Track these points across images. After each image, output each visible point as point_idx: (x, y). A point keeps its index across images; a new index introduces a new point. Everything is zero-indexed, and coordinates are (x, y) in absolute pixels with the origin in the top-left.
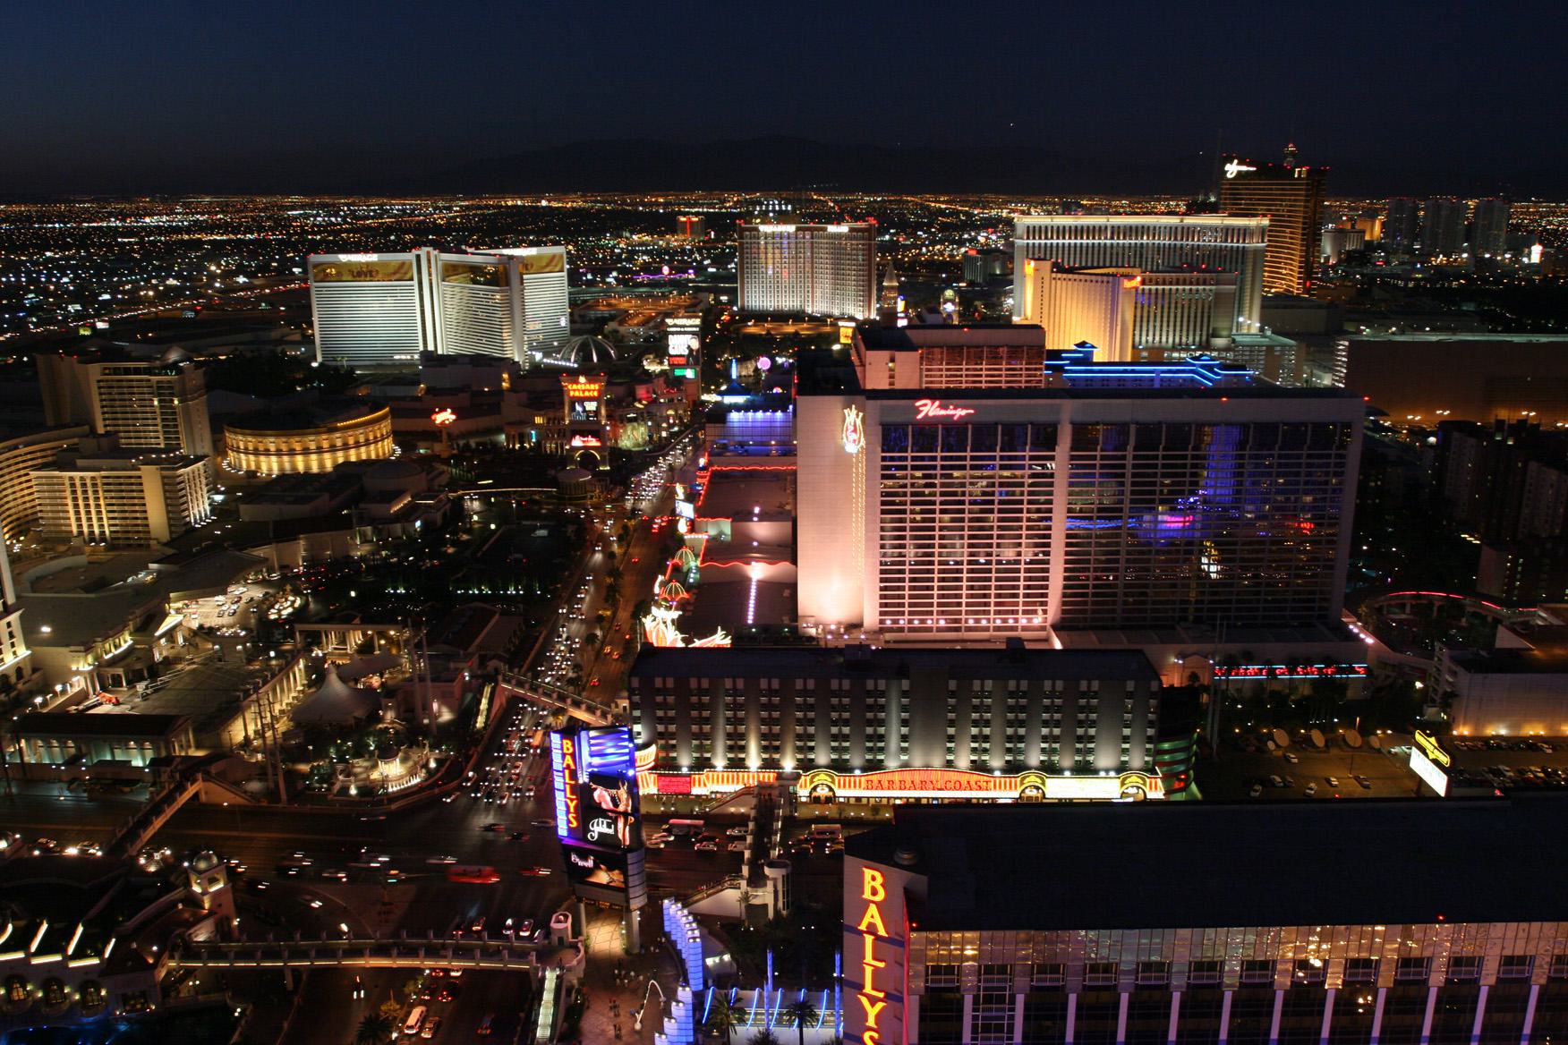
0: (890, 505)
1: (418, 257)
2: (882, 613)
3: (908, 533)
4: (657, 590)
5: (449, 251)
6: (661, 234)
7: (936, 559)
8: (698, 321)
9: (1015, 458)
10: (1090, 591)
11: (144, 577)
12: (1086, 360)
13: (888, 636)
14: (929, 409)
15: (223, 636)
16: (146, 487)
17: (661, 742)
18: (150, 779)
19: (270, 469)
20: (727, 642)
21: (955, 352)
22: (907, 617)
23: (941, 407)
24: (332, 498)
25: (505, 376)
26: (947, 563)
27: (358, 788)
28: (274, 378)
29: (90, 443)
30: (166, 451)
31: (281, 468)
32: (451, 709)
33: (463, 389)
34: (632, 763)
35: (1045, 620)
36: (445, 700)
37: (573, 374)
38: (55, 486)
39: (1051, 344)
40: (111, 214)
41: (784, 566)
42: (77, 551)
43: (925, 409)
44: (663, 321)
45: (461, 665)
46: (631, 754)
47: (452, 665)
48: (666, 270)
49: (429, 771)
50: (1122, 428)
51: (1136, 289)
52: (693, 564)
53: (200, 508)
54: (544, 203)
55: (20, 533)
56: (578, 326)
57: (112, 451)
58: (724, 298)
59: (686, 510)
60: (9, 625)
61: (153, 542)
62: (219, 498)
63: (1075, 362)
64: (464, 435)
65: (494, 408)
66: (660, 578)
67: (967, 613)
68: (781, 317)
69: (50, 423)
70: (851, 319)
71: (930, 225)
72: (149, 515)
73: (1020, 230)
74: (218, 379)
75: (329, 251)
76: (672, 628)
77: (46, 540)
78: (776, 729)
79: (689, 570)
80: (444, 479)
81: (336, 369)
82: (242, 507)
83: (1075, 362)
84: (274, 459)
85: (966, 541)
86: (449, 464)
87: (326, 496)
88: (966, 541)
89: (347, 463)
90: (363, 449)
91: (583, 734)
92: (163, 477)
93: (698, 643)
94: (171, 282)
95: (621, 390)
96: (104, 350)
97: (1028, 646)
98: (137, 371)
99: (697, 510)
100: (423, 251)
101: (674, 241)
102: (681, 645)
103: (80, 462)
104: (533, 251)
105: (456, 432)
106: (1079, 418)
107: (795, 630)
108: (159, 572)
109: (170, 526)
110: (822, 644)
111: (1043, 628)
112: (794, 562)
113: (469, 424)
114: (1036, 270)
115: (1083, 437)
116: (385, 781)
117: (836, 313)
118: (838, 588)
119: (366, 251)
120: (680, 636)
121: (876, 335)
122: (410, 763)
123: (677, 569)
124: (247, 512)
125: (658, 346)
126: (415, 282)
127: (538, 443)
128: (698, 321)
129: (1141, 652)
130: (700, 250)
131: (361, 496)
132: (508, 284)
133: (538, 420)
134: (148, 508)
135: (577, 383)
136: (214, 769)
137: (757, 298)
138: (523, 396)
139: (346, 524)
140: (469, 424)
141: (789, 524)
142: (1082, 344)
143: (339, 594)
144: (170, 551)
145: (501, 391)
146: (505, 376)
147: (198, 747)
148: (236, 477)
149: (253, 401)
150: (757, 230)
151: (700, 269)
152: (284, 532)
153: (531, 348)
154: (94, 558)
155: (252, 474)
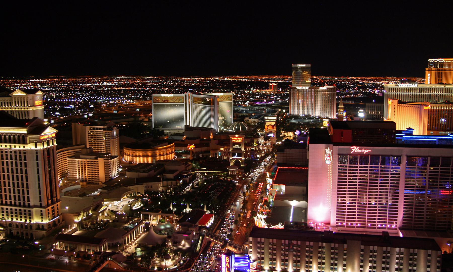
0: (341, 182)
1: (186, 95)
2: (337, 220)
3: (347, 192)
4: (259, 207)
5: (195, 94)
6: (264, 89)
7: (357, 202)
8: (275, 118)
9: (386, 168)
10: (413, 216)
11: (96, 193)
12: (411, 134)
13: (339, 228)
15: (118, 214)
16: (99, 165)
17: (258, 261)
18: (94, 258)
19: (136, 161)
20: (282, 227)
22: (346, 222)
23: (359, 149)
24: (155, 171)
25: (211, 134)
26: (361, 204)
27: (158, 268)
28: (140, 132)
30: (106, 154)
31: (140, 161)
32: (188, 243)
33: (198, 138)
34: (249, 267)
35: (396, 226)
36: (187, 240)
37: (233, 134)
38: (73, 163)
39: (397, 129)
40: (95, 82)
41: (303, 203)
42: (78, 184)
43: (354, 150)
44: (264, 118)
45: (193, 229)
46: (249, 264)
47: (190, 229)
48: (265, 100)
49: (180, 264)
50: (425, 158)
51: (429, 109)
52: (271, 200)
53: (115, 172)
54: (226, 79)
55: (63, 177)
56: (235, 119)
57: (90, 153)
58: (284, 111)
59: (270, 181)
60: (57, 205)
61: (100, 182)
62: (120, 170)
63: (406, 134)
64: (198, 153)
65: (208, 145)
66: (260, 204)
67: (368, 222)
69: (74, 144)
70: (327, 118)
71: (354, 87)
72: (100, 174)
75: (159, 93)
76: (263, 221)
77: (70, 180)
78: (299, 259)
79: (270, 202)
80: (190, 167)
81: (158, 130)
82: (127, 173)
83: (406, 134)
84: (138, 158)
85: (368, 196)
86: (192, 162)
87: (153, 171)
88: (368, 196)
89: (160, 161)
90: (165, 156)
91: (233, 256)
92: (105, 162)
93: (272, 227)
94: (111, 102)
95: (249, 140)
96: (90, 122)
97: (390, 235)
98: (100, 129)
99: (273, 181)
100: (188, 94)
101: (268, 92)
102: (266, 227)
103: (81, 156)
104: (222, 94)
105: (194, 151)
106: (409, 154)
107: (306, 224)
108: (101, 192)
109: (105, 178)
110: (316, 230)
111: (396, 229)
112: (307, 200)
113: (199, 149)
114: (392, 103)
115: (411, 161)
116: (166, 267)
117: (322, 116)
118: (322, 211)
119: (170, 93)
120: (266, 224)
122: (174, 261)
123: (266, 201)
124: (128, 175)
125: (262, 126)
126: (184, 103)
127: (221, 157)
128: (275, 118)
129: (433, 240)
130: (276, 95)
131: (164, 171)
132: (214, 104)
133: (222, 149)
134: (100, 171)
135: (235, 137)
136: (113, 257)
137: (294, 111)
139: (158, 180)
140: (199, 149)
141: (305, 188)
142: (409, 128)
144: (105, 186)
145: (209, 139)
146: (211, 134)
147: (109, 249)
148: (125, 163)
149: (132, 140)
150: (296, 88)
151: (276, 100)
152: (139, 181)
153: (220, 125)
154: (82, 187)
155: (131, 162)
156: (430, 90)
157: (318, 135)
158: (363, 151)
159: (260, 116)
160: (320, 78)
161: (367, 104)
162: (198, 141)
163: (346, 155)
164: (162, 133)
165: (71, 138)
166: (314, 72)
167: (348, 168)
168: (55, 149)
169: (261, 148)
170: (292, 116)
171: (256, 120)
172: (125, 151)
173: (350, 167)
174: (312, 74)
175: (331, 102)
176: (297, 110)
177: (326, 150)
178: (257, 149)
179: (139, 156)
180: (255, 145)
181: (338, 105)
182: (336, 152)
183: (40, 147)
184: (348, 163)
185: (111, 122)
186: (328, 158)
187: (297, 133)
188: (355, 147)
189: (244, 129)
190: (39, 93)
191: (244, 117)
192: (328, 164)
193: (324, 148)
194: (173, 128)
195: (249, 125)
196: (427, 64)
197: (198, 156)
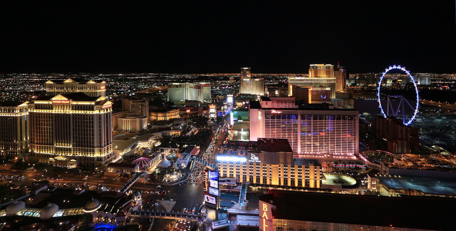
14: (274, 111)
21: (278, 102)
29: (128, 114)
37: (211, 104)
53: (145, 126)
65: (197, 110)
68: (247, 95)
73: (289, 80)
74: (151, 103)
89: (171, 119)
113: (192, 112)
117: (257, 94)
121: (264, 98)
124: (153, 127)
125: (225, 99)
138: (202, 108)
140: (192, 112)
143: (167, 142)
152: (160, 130)
156: (311, 80)
157: (254, 104)
158: (277, 112)
159: (225, 94)
160: (255, 75)
161: (280, 88)
162: (192, 108)
164: (173, 104)
165: (121, 107)
166: (252, 71)
168: (111, 114)
170: (241, 94)
171: (223, 97)
172: (153, 114)
174: (251, 73)
175: (261, 87)
176: (244, 91)
179: (160, 116)
181: (264, 88)
183: (102, 112)
185: (144, 99)
186: (260, 116)
187: (244, 103)
189: (216, 101)
190: (104, 82)
191: (216, 95)
194: (179, 101)
195: (219, 99)
196: (309, 67)
197: (192, 116)
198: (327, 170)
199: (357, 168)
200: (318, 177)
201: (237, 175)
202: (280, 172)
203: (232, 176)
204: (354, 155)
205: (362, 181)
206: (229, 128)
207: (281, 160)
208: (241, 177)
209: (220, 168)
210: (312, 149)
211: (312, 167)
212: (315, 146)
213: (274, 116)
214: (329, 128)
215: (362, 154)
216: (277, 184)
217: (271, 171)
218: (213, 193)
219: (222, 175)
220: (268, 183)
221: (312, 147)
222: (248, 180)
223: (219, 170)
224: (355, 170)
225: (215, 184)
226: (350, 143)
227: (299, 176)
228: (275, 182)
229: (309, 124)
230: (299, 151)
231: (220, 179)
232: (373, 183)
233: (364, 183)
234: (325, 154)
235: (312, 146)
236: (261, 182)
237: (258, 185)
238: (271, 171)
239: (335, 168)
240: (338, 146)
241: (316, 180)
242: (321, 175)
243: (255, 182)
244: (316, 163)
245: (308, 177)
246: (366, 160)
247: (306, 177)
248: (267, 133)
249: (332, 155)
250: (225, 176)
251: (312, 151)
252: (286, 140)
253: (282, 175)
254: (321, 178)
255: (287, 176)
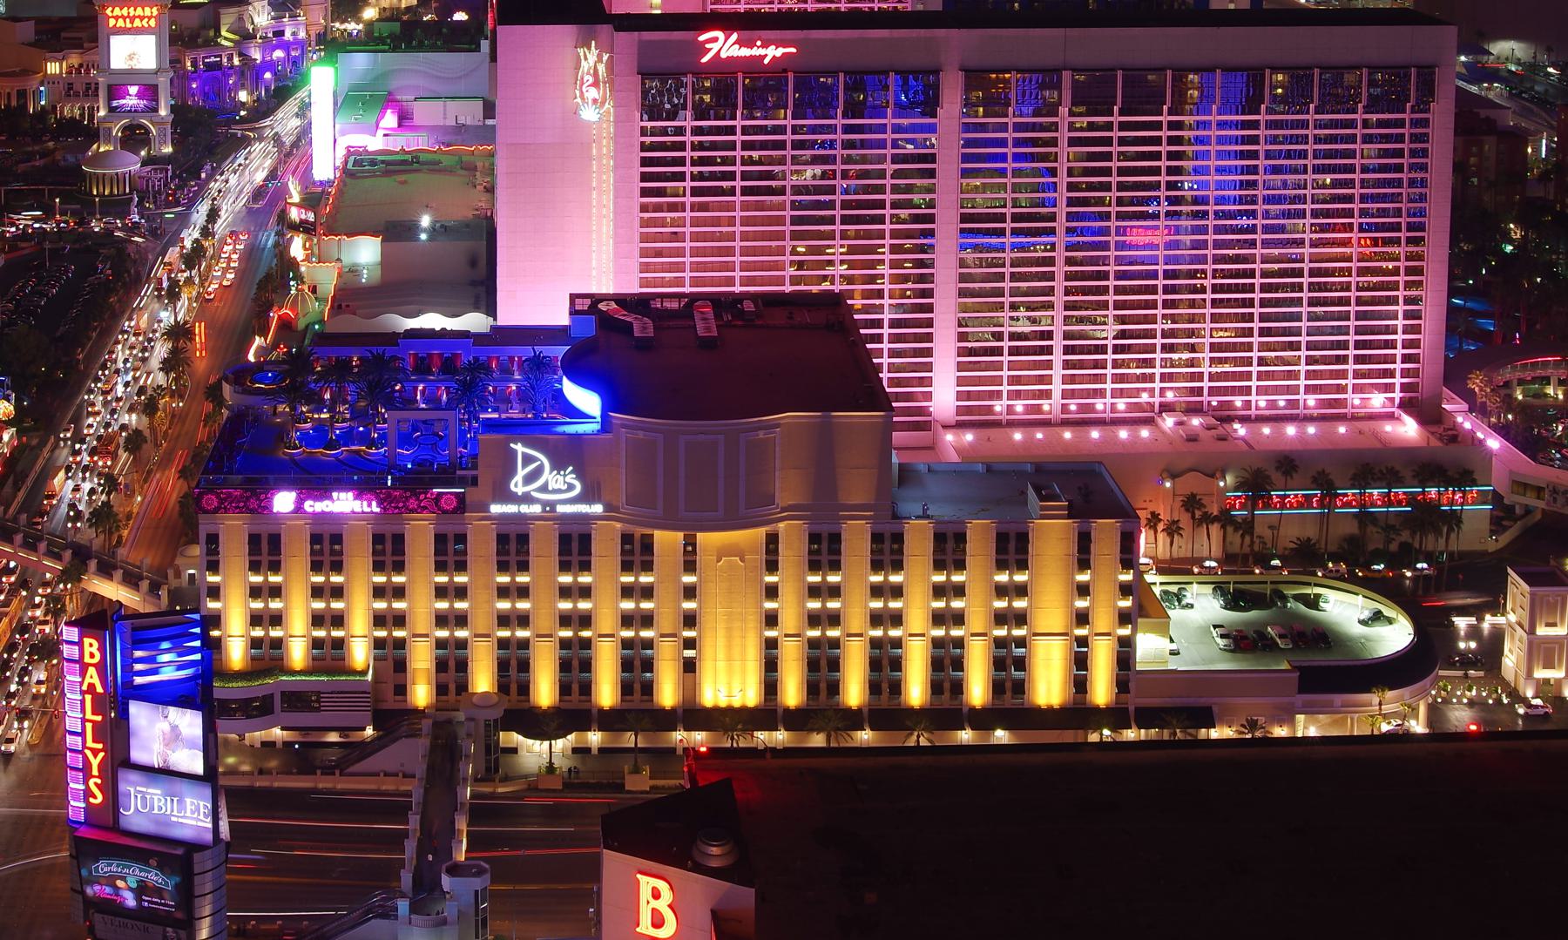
14: (723, 46)
43: (715, 47)
133: (53, 68)
138: (27, 30)
158: (756, 52)
163: (677, 75)
167: (688, 138)
169: (256, 55)
173: (698, 131)
177: (581, 51)
178: (236, 61)
180: (226, 37)
182: (630, 61)
184: (689, 114)
186: (592, 93)
188: (720, 34)
192: (588, 124)
193: (570, 41)
198: (1182, 548)
199: (1429, 517)
200: (1105, 609)
201: (379, 644)
202: (772, 592)
203: (330, 655)
204: (1405, 405)
205: (1462, 623)
206: (295, 214)
207: (788, 487)
208: (421, 658)
209: (214, 592)
210: (1057, 372)
211: (1052, 536)
212: (1082, 352)
213: (727, 89)
214: (1207, 178)
215: (1468, 396)
216: (748, 694)
217: (690, 592)
218: (164, 820)
219: (236, 654)
220: (667, 695)
221: (1058, 357)
222: (483, 681)
223: (212, 605)
224: (1405, 536)
225: (174, 737)
226: (1377, 298)
227: (938, 619)
228: (730, 682)
229: (1036, 150)
230: (944, 397)
231: (220, 688)
232: (1542, 631)
233: (1474, 632)
234: (1166, 408)
235: (1058, 343)
236: (606, 694)
237: (574, 711)
238: (690, 592)
239: (1247, 526)
240: (1279, 331)
241: (1083, 642)
242: (1125, 590)
243: (545, 692)
244: (1090, 493)
245: (1021, 618)
246: (1494, 443)
247: (1000, 618)
248: (655, 245)
249: (1225, 416)
250: (268, 656)
251: (1057, 387)
252: (835, 301)
253: (790, 620)
254: (1125, 618)
255: (834, 619)
